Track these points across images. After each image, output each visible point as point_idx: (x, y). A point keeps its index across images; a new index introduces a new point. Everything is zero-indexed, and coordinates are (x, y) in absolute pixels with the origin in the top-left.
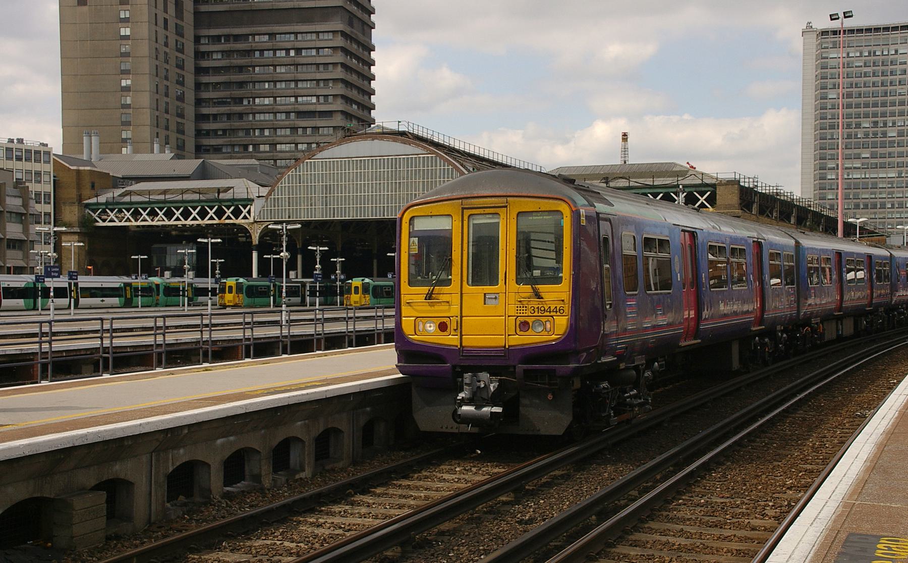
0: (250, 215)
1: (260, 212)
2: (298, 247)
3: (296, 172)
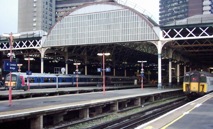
0: (40, 44)
1: (45, 42)
2: (66, 61)
3: (60, 23)
